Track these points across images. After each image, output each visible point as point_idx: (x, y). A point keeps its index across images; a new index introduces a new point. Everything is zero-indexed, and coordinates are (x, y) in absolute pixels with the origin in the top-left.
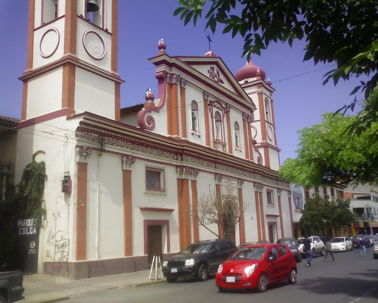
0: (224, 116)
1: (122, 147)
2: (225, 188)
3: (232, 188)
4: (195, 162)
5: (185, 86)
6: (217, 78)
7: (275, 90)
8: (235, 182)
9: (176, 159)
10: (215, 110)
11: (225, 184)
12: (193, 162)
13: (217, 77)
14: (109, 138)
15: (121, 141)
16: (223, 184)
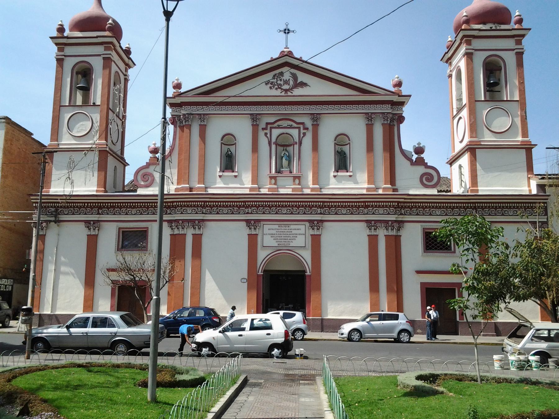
0: (304, 134)
1: (86, 214)
2: (271, 237)
3: (291, 236)
4: (200, 213)
5: (204, 122)
6: (289, 85)
7: (530, 29)
8: (302, 228)
9: (169, 214)
10: (276, 132)
11: (274, 232)
12: (197, 213)
13: (291, 83)
14: (70, 209)
15: (83, 209)
16: (266, 231)
